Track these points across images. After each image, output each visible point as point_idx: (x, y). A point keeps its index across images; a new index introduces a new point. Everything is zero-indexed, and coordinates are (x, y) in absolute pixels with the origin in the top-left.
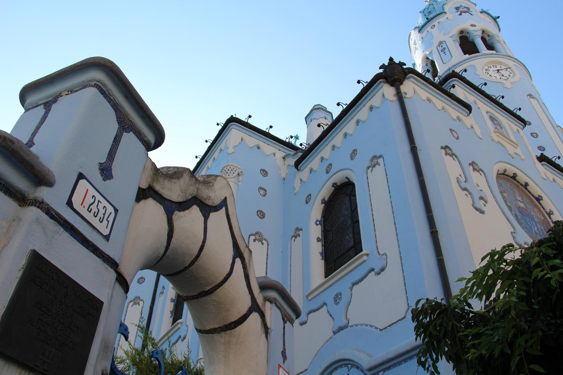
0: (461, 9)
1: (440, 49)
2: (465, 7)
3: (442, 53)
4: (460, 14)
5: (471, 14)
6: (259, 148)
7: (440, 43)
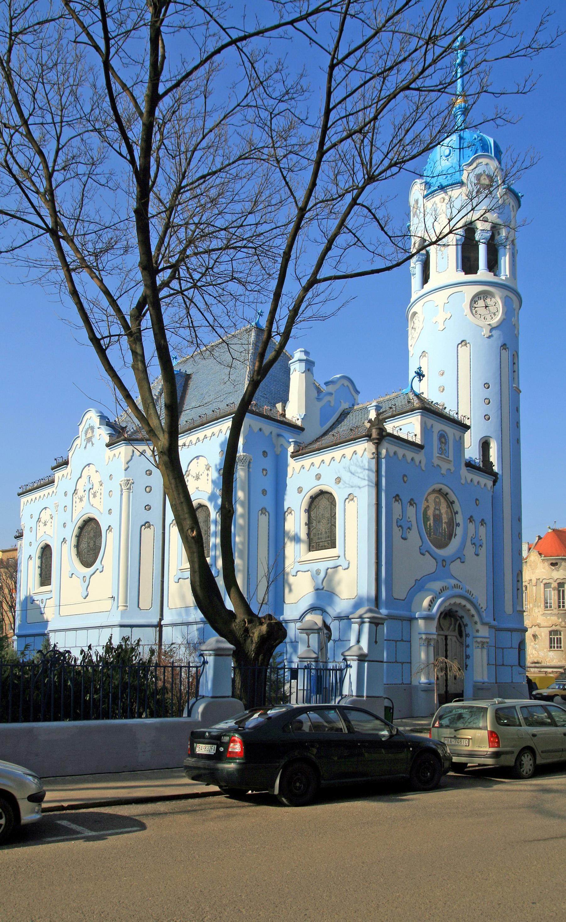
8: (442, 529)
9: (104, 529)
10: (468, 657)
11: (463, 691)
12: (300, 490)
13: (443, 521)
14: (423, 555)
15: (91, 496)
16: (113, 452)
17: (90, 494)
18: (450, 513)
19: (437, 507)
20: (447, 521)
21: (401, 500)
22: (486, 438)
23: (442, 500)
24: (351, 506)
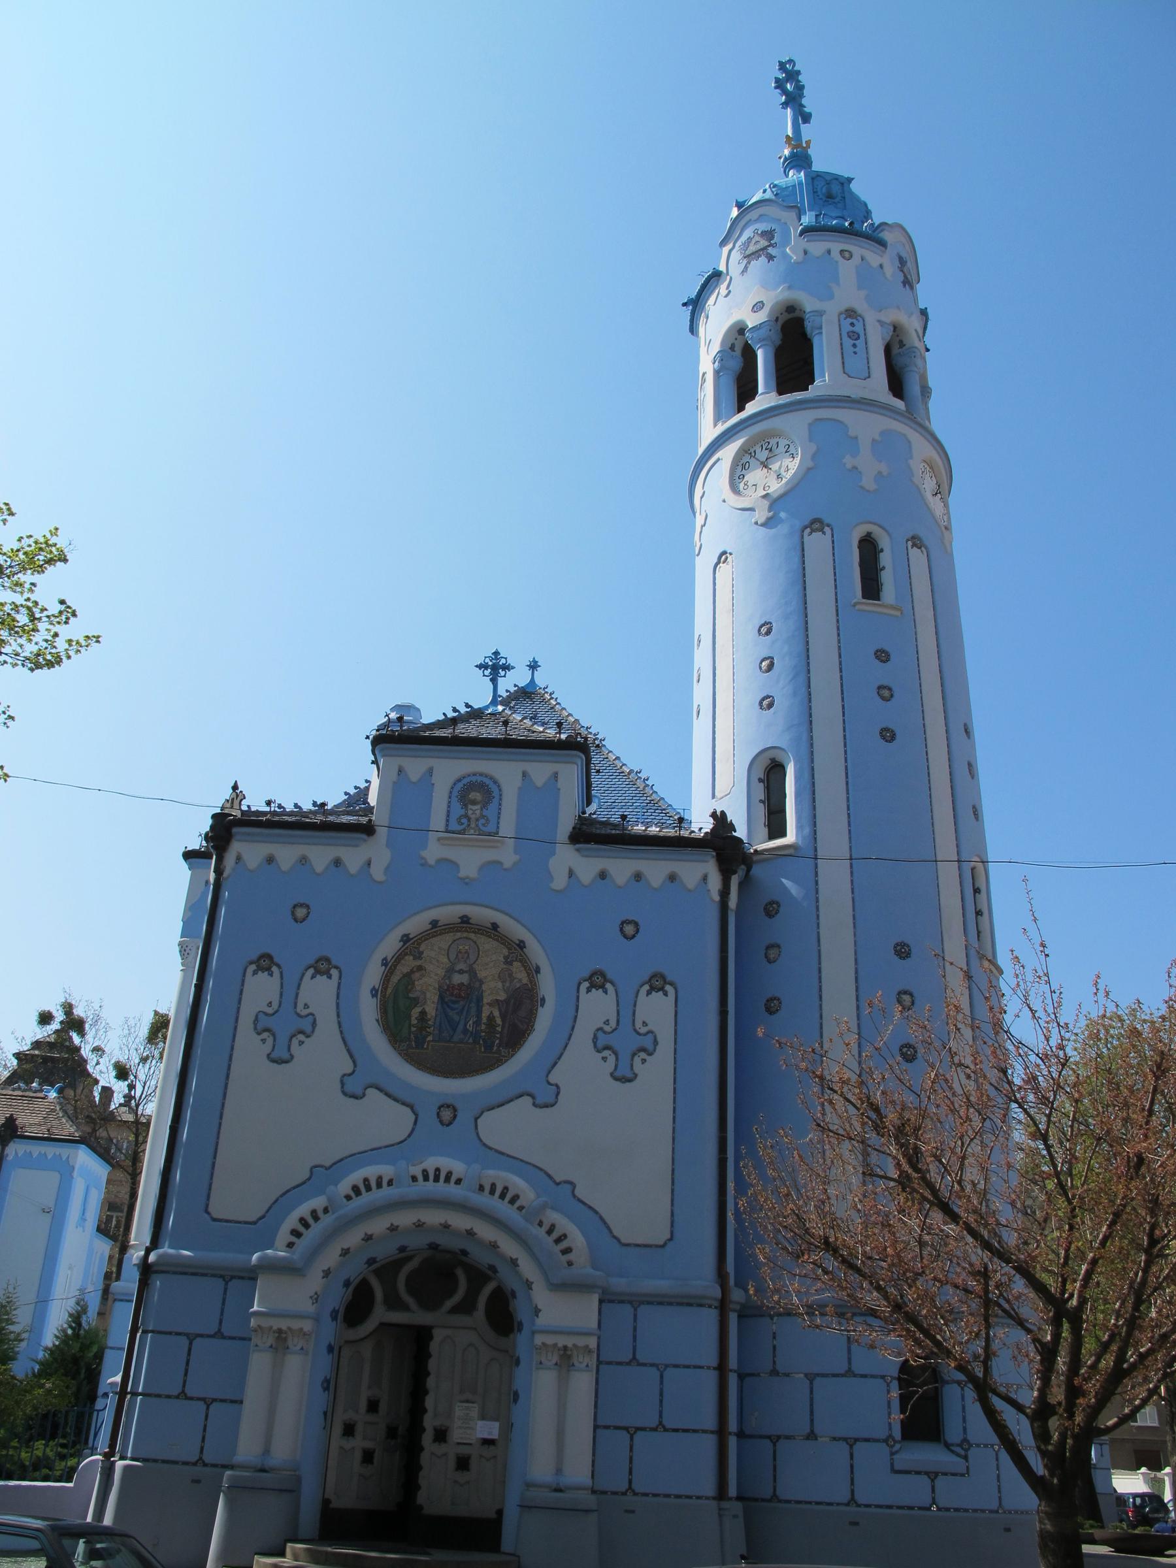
5: (771, 258)
8: (478, 1023)
10: (516, 1397)
11: (500, 1513)
13: (485, 1001)
18: (521, 975)
19: (461, 966)
20: (502, 996)
21: (279, 966)
22: (771, 754)
23: (486, 944)
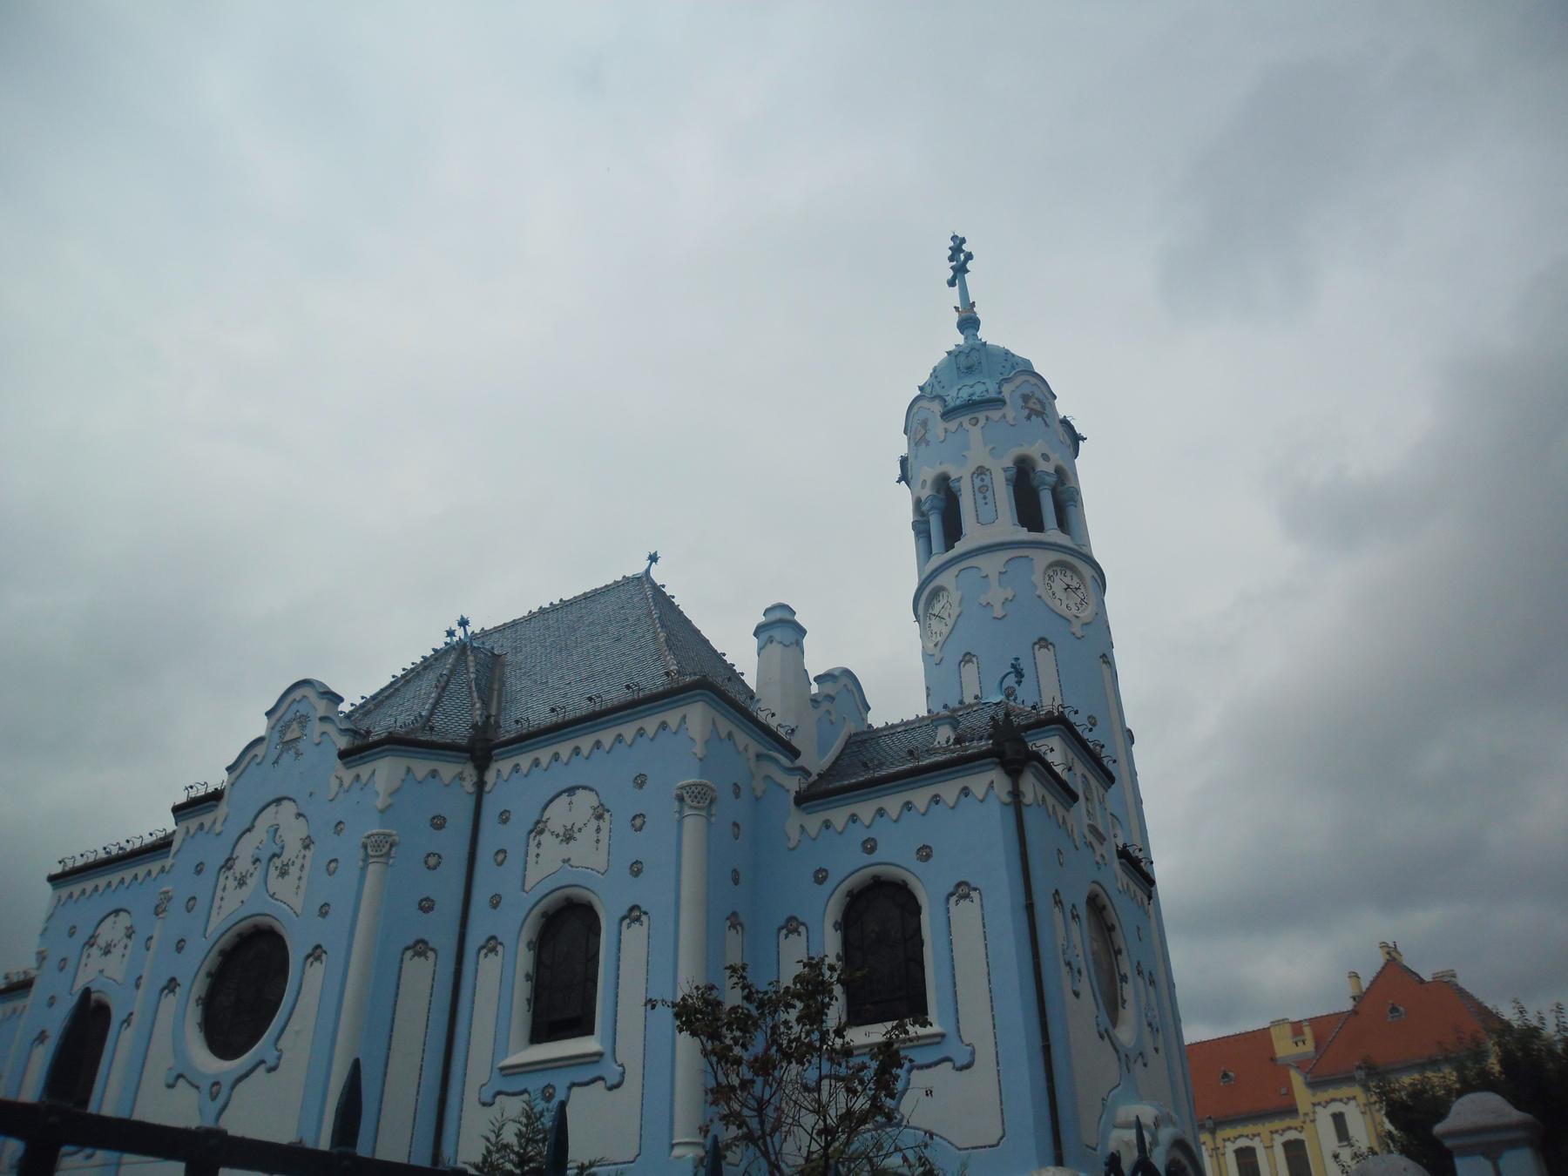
0: (1030, 405)
1: (978, 483)
2: (1040, 401)
3: (979, 496)
4: (1028, 418)
6: (730, 735)
7: (981, 471)
9: (296, 953)
12: (821, 876)
14: (1102, 1037)
15: (273, 873)
16: (354, 771)
17: (272, 869)
24: (966, 914)
